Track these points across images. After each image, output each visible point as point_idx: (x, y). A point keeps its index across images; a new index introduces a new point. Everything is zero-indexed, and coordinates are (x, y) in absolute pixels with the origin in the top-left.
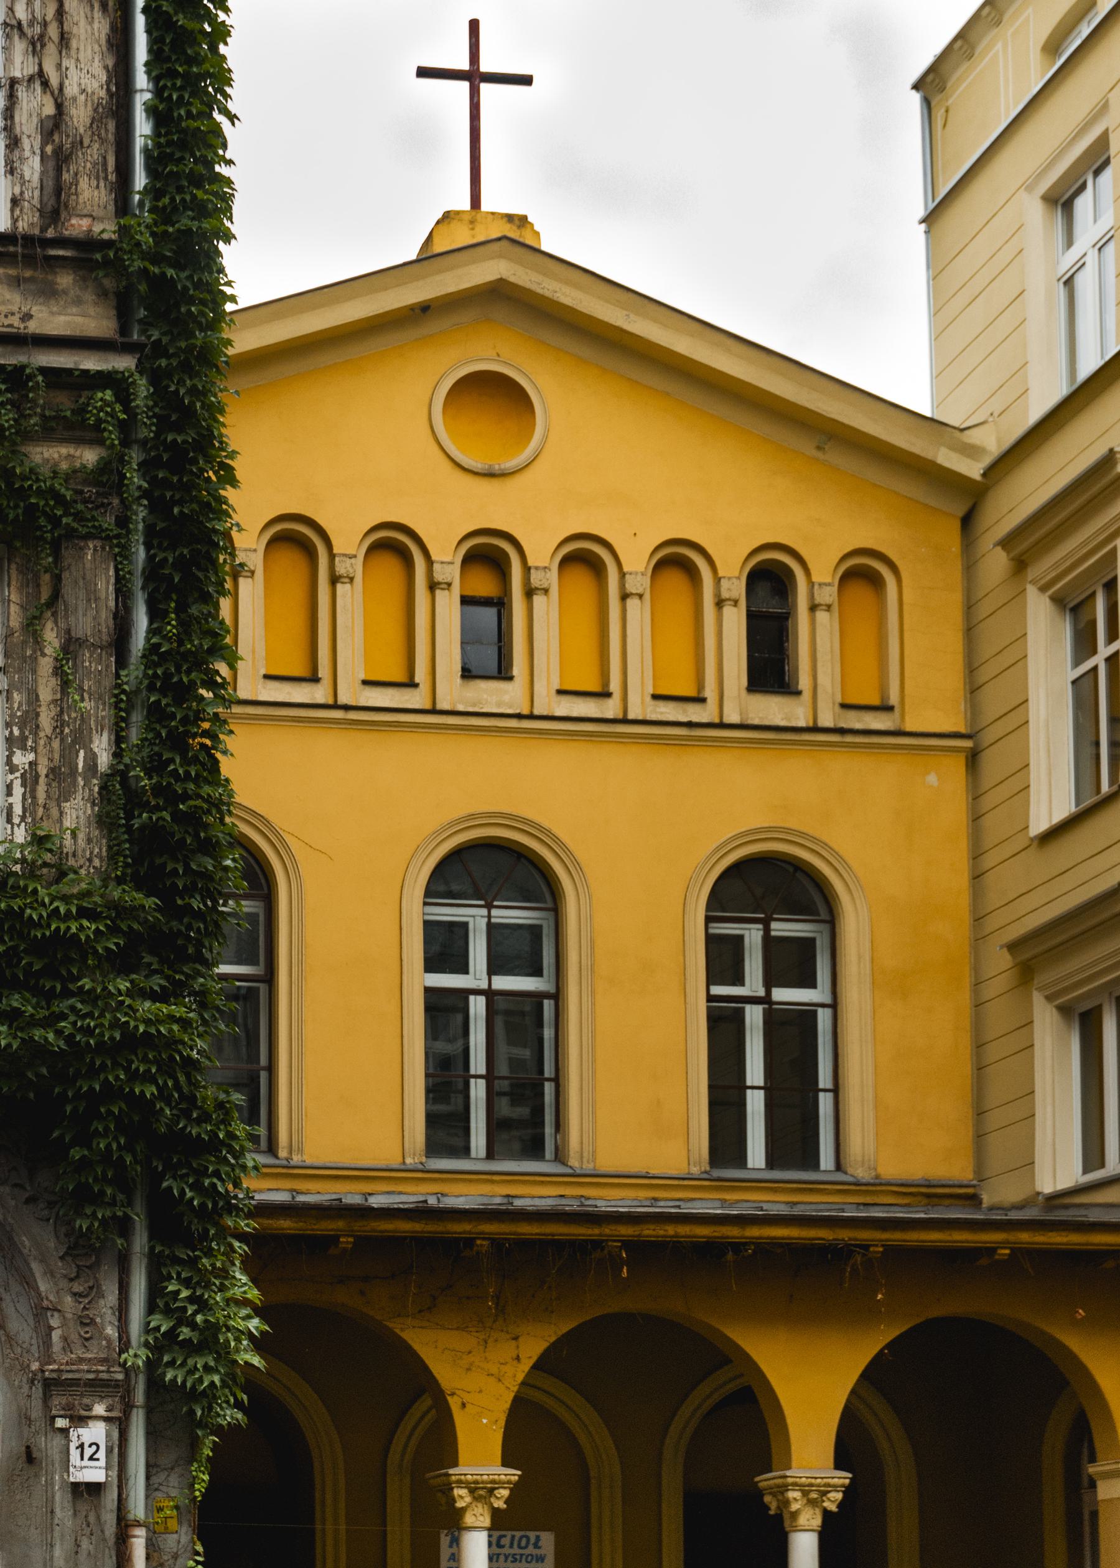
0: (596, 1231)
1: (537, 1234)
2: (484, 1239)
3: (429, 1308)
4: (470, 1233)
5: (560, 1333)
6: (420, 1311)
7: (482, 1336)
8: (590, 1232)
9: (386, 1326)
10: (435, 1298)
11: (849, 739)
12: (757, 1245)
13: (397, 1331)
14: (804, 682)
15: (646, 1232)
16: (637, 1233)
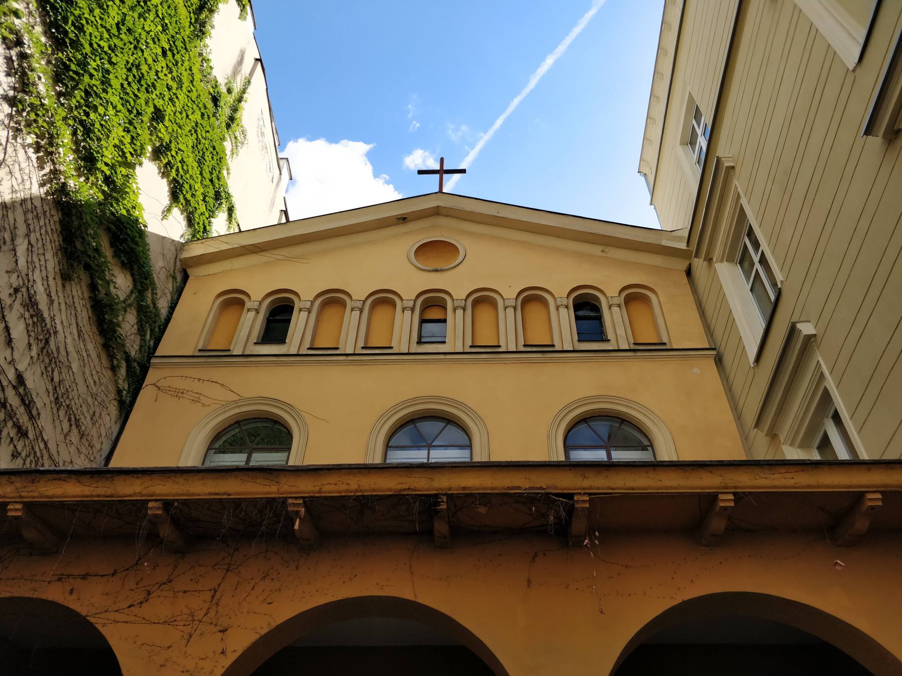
0: (274, 489)
1: (210, 494)
2: (156, 500)
3: (141, 603)
4: (140, 494)
5: (274, 625)
6: (130, 607)
7: (188, 629)
8: (267, 489)
9: (88, 621)
10: (149, 593)
11: (639, 354)
12: (450, 496)
13: (99, 627)
14: (610, 335)
15: (327, 488)
16: (317, 488)
